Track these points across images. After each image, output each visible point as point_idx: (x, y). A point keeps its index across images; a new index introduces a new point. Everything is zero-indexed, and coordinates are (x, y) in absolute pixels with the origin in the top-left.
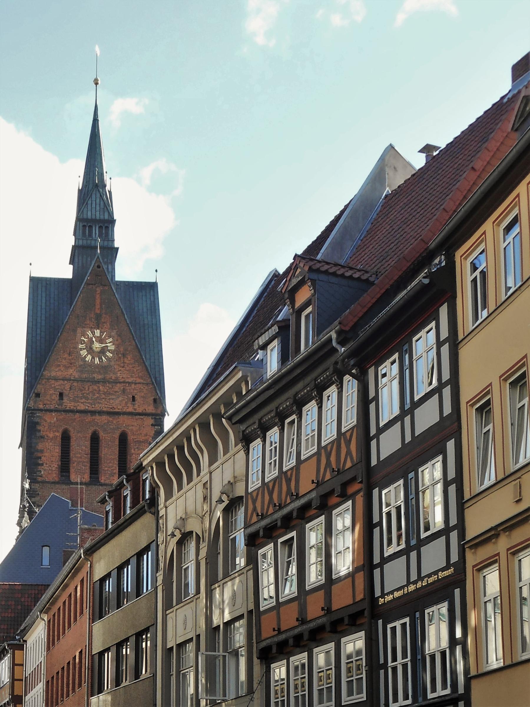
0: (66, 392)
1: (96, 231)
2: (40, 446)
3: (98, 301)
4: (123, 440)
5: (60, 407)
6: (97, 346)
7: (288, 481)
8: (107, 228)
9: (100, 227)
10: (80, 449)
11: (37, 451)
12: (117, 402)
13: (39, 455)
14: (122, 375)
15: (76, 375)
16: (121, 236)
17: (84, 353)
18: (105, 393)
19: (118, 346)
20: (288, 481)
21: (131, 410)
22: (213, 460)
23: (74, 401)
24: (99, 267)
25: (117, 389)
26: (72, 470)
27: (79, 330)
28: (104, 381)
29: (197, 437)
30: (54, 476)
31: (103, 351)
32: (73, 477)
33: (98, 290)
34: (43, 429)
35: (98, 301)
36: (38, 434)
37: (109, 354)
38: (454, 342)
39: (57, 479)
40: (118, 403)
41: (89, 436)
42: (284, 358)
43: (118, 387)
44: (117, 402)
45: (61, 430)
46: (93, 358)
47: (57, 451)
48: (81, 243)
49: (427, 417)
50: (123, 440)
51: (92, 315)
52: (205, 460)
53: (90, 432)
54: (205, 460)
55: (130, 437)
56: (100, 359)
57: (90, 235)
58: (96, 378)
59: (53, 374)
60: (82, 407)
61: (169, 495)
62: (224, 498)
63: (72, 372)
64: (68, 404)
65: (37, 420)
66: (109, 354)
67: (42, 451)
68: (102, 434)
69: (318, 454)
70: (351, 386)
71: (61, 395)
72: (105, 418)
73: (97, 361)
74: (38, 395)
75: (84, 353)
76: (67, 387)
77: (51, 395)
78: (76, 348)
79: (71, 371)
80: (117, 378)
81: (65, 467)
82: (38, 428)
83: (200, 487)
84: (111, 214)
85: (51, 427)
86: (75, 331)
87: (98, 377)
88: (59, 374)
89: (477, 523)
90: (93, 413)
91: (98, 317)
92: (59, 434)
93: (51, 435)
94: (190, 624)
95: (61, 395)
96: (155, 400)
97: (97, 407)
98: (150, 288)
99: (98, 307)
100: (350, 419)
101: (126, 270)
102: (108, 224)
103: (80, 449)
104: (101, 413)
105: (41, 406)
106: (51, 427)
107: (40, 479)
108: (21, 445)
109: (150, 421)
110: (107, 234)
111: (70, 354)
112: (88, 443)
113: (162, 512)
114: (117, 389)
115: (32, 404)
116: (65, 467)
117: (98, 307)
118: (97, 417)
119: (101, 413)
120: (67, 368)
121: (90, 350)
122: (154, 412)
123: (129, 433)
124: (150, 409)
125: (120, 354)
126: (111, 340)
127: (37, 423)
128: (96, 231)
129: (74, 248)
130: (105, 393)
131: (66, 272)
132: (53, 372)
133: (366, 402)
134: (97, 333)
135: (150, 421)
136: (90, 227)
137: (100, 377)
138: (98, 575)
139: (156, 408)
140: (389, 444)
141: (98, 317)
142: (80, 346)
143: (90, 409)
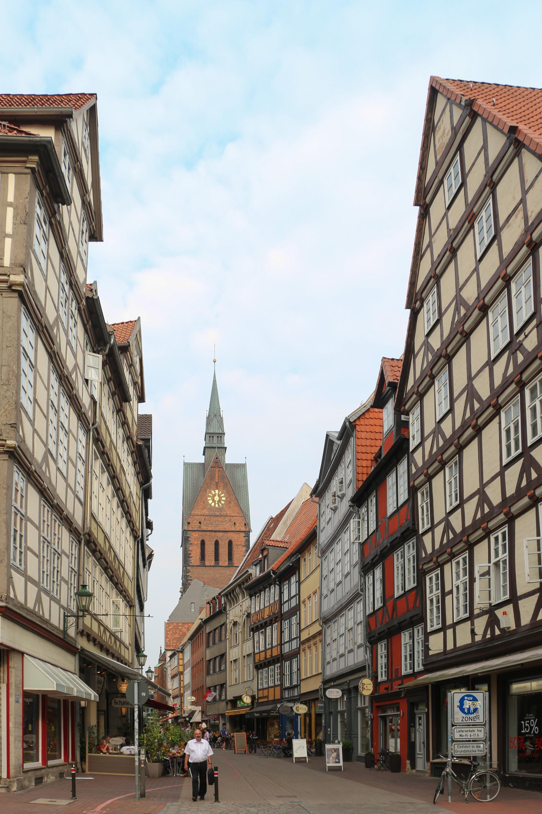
0: (202, 522)
1: (215, 438)
2: (190, 548)
3: (217, 475)
4: (230, 543)
5: (199, 529)
6: (217, 498)
7: (262, 613)
8: (221, 437)
9: (218, 437)
10: (210, 549)
11: (189, 551)
12: (227, 526)
13: (190, 552)
14: (229, 512)
15: (207, 513)
16: (228, 441)
17: (210, 502)
18: (221, 522)
19: (227, 498)
20: (262, 613)
21: (233, 529)
22: (243, 597)
23: (206, 526)
24: (217, 458)
25: (226, 519)
26: (206, 560)
27: (208, 491)
28: (220, 516)
29: (238, 590)
30: (198, 563)
31: (219, 501)
32: (207, 563)
33: (217, 470)
34: (192, 540)
35: (217, 475)
36: (189, 542)
37: (223, 502)
38: (299, 582)
39: (199, 564)
40: (227, 526)
41: (214, 543)
42: (260, 572)
43: (227, 519)
44: (227, 526)
45: (200, 540)
46: (215, 504)
47: (199, 550)
48: (208, 445)
49: (294, 603)
50: (230, 543)
51: (214, 483)
52: (241, 597)
53: (214, 541)
54: (241, 597)
55: (234, 543)
56: (218, 504)
57: (213, 441)
58: (217, 514)
59: (196, 513)
60: (210, 529)
61: (230, 606)
62: (246, 613)
63: (206, 512)
64: (204, 528)
65: (188, 535)
66: (223, 502)
67: (191, 551)
68: (220, 542)
69: (269, 606)
70: (277, 587)
71: (200, 523)
72: (221, 534)
73: (217, 506)
74: (189, 523)
75: (210, 502)
76: (203, 519)
77: (195, 523)
78: (207, 499)
79: (204, 511)
80: (227, 514)
81: (203, 557)
82: (189, 539)
83: (239, 606)
84: (223, 430)
85: (195, 539)
86: (206, 491)
87: (218, 514)
88: (199, 512)
89: (305, 636)
90: (215, 531)
91: (217, 484)
92: (199, 542)
93: (196, 543)
94: (237, 654)
95: (200, 523)
96: (245, 524)
97: (218, 529)
98: (242, 467)
99: (217, 478)
100: (277, 598)
101: (230, 458)
102: (221, 435)
103: (210, 549)
104: (219, 531)
105: (191, 529)
106: (195, 539)
107: (191, 564)
108: (182, 546)
109: (243, 534)
110: (221, 441)
111: (204, 502)
112: (213, 546)
113: (228, 612)
114: (226, 519)
115: (186, 528)
116: (203, 557)
117: (217, 478)
118: (217, 533)
119: (219, 531)
120: (202, 509)
121: (214, 501)
122: (245, 530)
123: (233, 541)
124: (243, 529)
125: (228, 502)
126: (223, 495)
127: (189, 537)
128: (215, 438)
129: (205, 447)
130: (221, 522)
131: (201, 459)
132: (196, 512)
133: (281, 593)
134: (217, 491)
135: (243, 534)
136: (213, 437)
137: (218, 513)
138: (208, 631)
139: (246, 528)
140: (286, 608)
141: (217, 484)
142: (209, 498)
143: (214, 530)
